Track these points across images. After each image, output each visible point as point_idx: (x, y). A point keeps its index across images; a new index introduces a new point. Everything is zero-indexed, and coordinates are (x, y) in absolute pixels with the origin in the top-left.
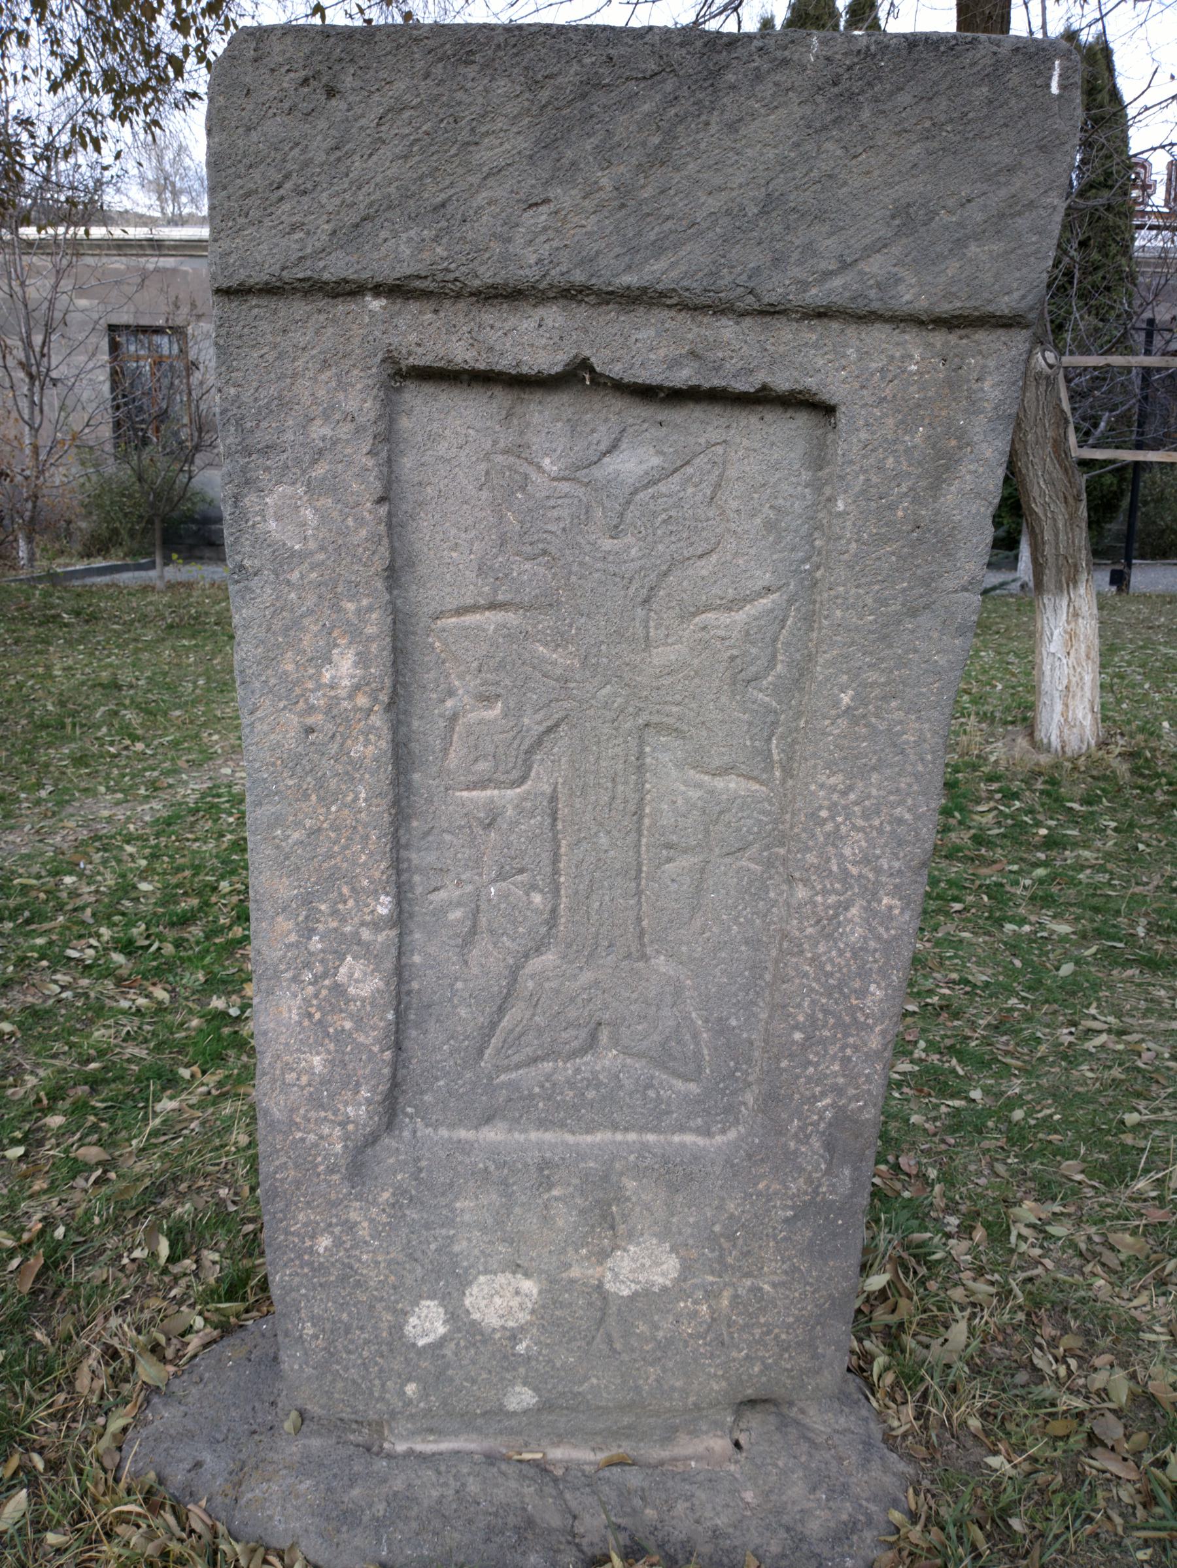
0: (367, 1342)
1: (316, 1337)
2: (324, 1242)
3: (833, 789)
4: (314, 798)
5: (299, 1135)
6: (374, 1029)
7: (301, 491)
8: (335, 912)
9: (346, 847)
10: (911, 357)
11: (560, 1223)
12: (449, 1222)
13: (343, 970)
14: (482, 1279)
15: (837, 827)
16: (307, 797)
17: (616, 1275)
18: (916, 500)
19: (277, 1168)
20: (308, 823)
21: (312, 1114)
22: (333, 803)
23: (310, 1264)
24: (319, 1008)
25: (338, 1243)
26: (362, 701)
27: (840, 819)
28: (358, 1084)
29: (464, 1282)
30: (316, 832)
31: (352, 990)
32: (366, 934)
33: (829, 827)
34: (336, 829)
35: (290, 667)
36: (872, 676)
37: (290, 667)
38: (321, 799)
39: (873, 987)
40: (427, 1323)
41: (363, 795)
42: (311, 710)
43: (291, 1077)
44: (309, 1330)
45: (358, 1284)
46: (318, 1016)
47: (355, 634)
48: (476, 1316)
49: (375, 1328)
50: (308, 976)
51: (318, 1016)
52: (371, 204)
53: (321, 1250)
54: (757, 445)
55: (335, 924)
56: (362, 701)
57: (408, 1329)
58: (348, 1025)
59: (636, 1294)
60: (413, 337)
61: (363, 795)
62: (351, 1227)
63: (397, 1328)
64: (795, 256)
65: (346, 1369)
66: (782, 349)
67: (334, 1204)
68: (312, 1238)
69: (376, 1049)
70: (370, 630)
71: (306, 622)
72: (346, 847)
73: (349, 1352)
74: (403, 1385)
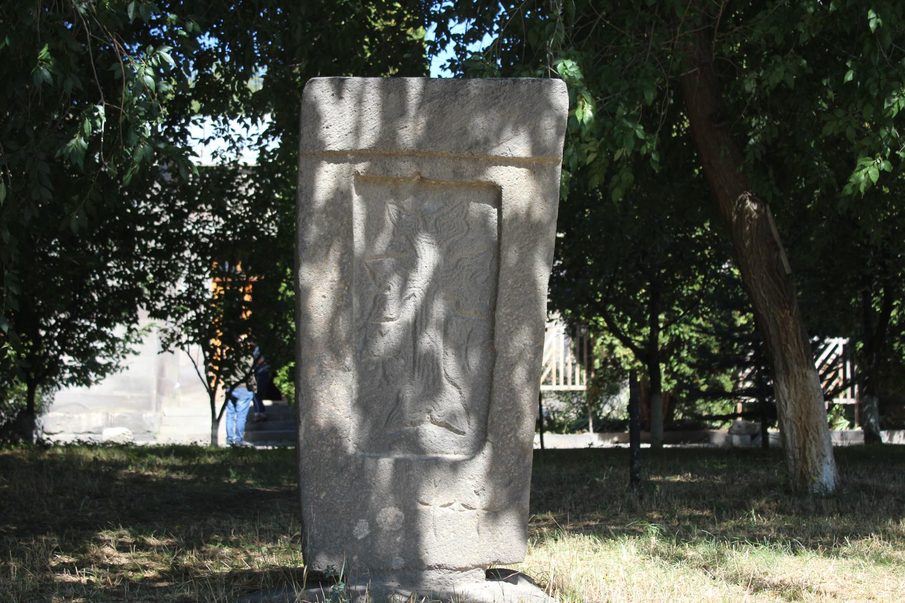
0: (338, 537)
1: (318, 535)
2: (323, 495)
3: (507, 315)
19: (305, 463)
36: (519, 274)
44: (316, 532)
68: (318, 493)
74: (352, 556)
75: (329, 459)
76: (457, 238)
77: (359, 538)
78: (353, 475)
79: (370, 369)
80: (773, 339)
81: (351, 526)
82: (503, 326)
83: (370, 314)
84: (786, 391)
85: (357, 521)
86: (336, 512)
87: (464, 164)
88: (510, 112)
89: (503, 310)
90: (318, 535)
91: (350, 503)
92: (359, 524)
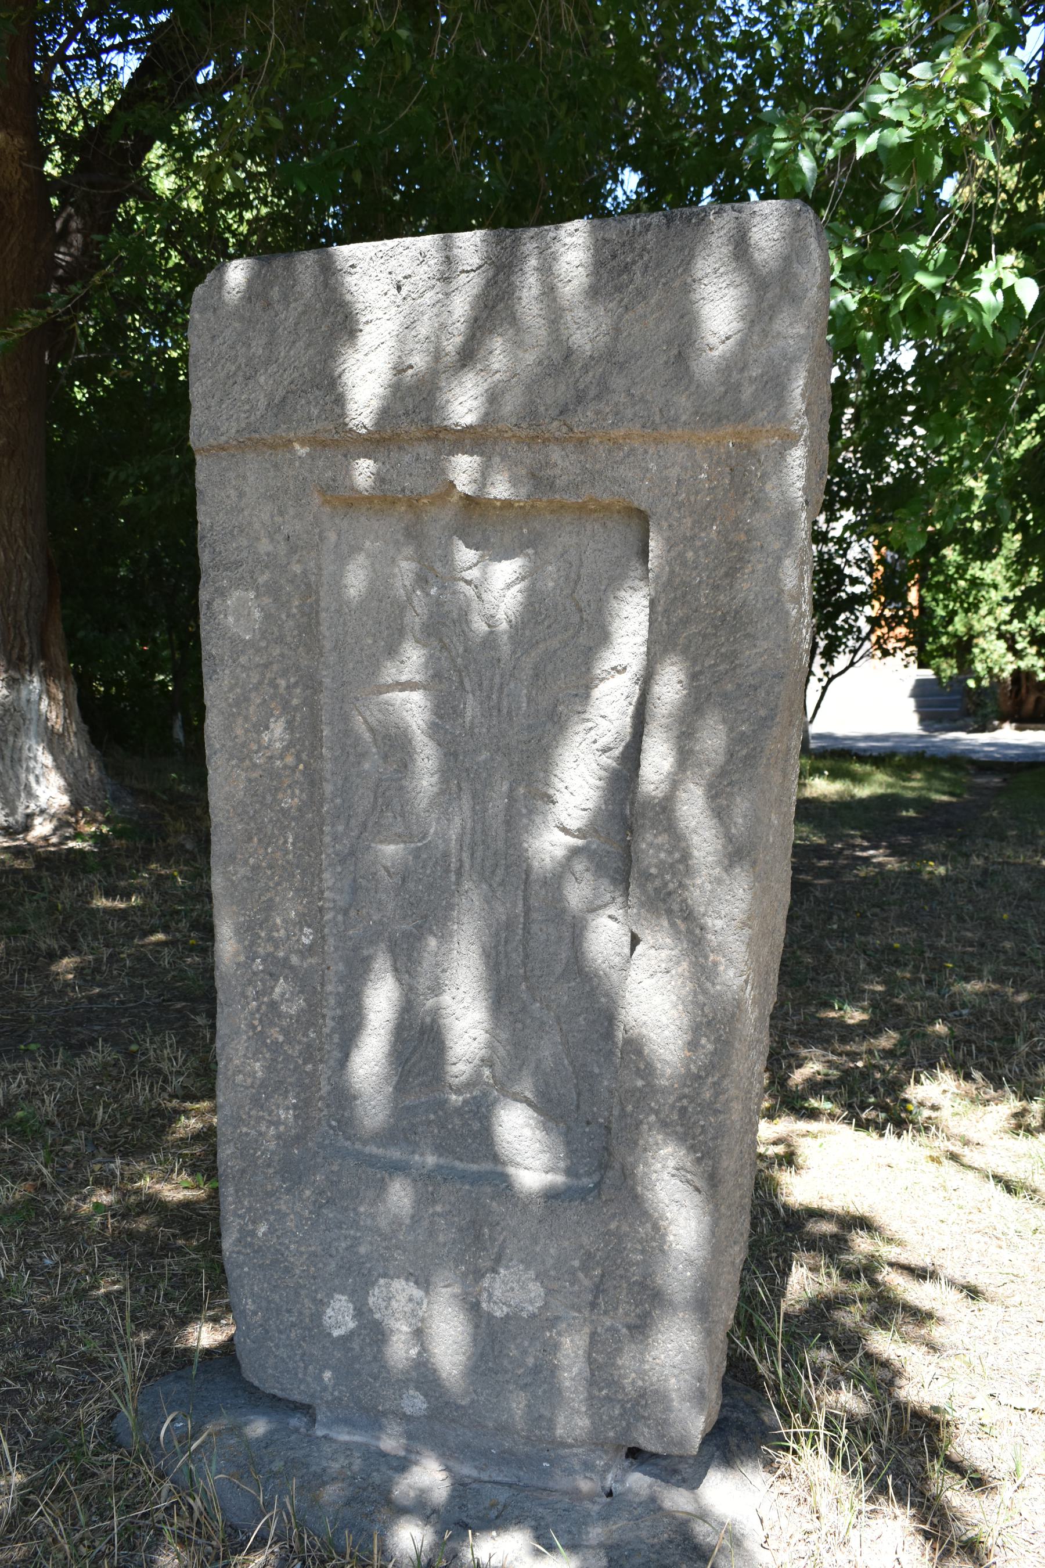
0: (293, 1325)
2: (262, 1229)
5: (244, 1130)
6: (299, 1042)
7: (252, 595)
8: (270, 939)
9: (278, 884)
10: (701, 468)
11: (441, 1238)
13: (277, 990)
14: (382, 1281)
15: (666, 884)
17: (490, 1296)
18: (716, 588)
20: (252, 861)
21: (253, 1113)
22: (268, 845)
23: (251, 1245)
24: (261, 1021)
25: (272, 1230)
26: (290, 760)
27: (668, 877)
28: (287, 1092)
29: (367, 1283)
30: (256, 868)
31: (284, 1008)
32: (295, 960)
35: (239, 732)
37: (239, 732)
38: (260, 840)
39: (703, 1041)
40: (340, 1316)
41: (290, 840)
42: (255, 765)
46: (259, 1028)
47: (286, 706)
48: (377, 1316)
49: (300, 1313)
50: (251, 992)
51: (259, 1028)
52: (292, 383)
53: (260, 1234)
54: (600, 546)
55: (272, 949)
56: (290, 760)
57: (327, 1321)
58: (281, 1038)
60: (329, 474)
61: (290, 840)
62: (282, 1216)
64: (593, 392)
65: (277, 1346)
66: (598, 466)
67: (269, 1194)
68: (254, 1222)
69: (300, 1062)
70: (295, 702)
71: (253, 695)
72: (278, 884)
73: (280, 1332)
74: (321, 1371)
75: (273, 1153)
76: (555, 643)
77: (336, 1333)
78: (322, 1193)
81: (322, 1304)
83: (364, 825)
85: (330, 1296)
86: (287, 1270)
87: (556, 454)
88: (659, 306)
89: (649, 837)
90: (255, 1313)
91: (314, 1254)
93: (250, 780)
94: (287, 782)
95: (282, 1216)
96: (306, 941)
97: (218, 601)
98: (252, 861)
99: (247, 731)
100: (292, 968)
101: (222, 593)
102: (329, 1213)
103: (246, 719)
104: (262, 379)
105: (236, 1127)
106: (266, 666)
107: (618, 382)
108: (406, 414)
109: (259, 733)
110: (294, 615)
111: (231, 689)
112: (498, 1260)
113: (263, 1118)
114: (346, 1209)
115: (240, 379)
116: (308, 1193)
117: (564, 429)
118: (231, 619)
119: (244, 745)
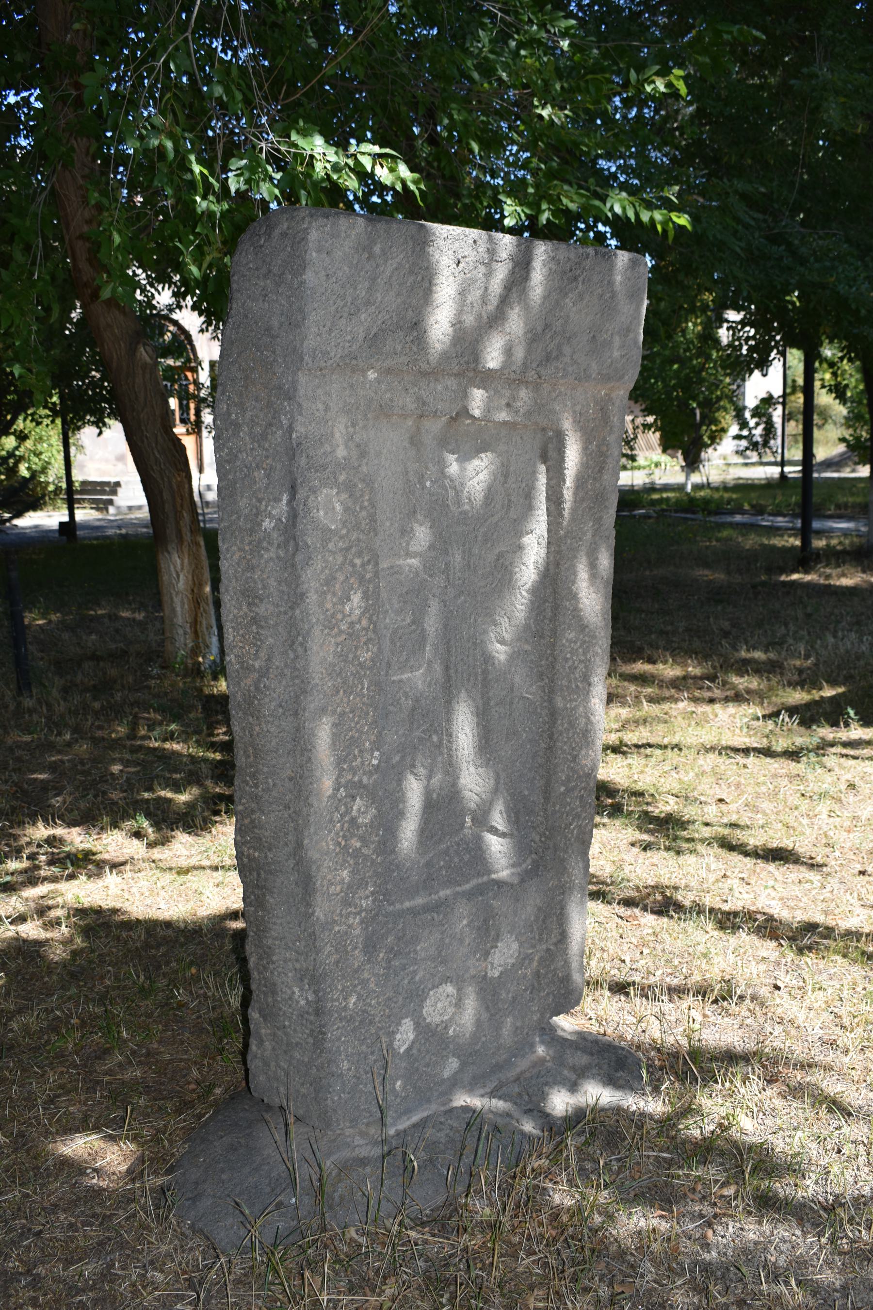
2: (353, 999)
4: (341, 692)
5: (337, 929)
9: (358, 723)
12: (415, 961)
14: (431, 993)
16: (338, 692)
17: (492, 964)
18: (595, 479)
20: (339, 709)
22: (351, 693)
24: (344, 837)
26: (364, 622)
30: (342, 714)
32: (365, 780)
33: (570, 663)
34: (352, 711)
37: (329, 605)
42: (341, 632)
43: (332, 889)
45: (371, 1022)
46: (343, 843)
47: (362, 580)
51: (343, 843)
58: (358, 845)
59: (501, 973)
60: (388, 395)
63: (390, 1045)
64: (554, 354)
68: (345, 999)
70: (368, 576)
72: (358, 723)
79: (394, 761)
80: (167, 506)
82: (566, 660)
84: (179, 561)
92: (402, 1029)
93: (337, 644)
94: (364, 640)
95: (364, 983)
96: (375, 762)
97: (312, 498)
98: (339, 709)
99: (334, 604)
100: (364, 787)
101: (314, 491)
102: (396, 963)
103: (334, 594)
104: (363, 317)
105: (331, 930)
106: (348, 549)
107: (567, 350)
108: (457, 357)
109: (344, 604)
110: (365, 508)
111: (322, 571)
112: (497, 938)
113: (350, 913)
114: (410, 952)
115: (345, 315)
116: (381, 955)
117: (536, 376)
118: (322, 513)
119: (333, 615)
